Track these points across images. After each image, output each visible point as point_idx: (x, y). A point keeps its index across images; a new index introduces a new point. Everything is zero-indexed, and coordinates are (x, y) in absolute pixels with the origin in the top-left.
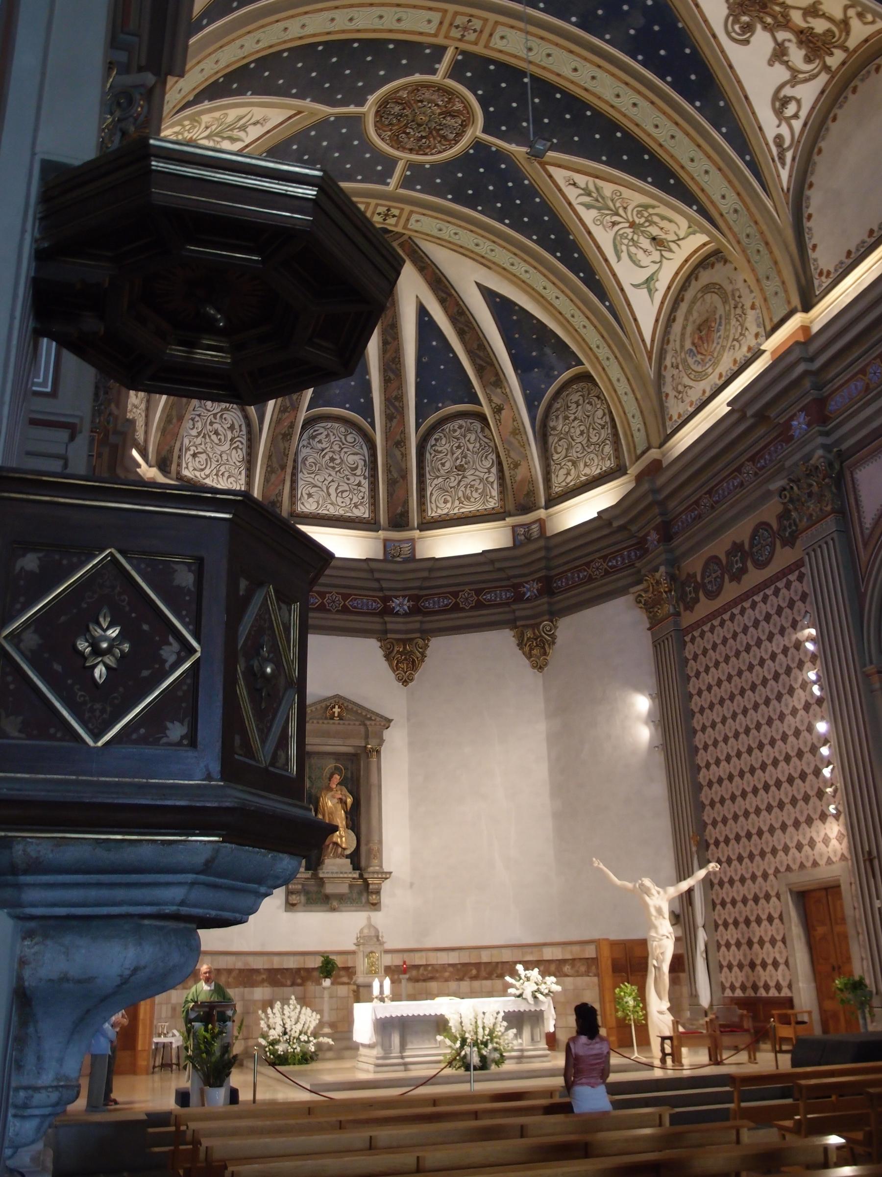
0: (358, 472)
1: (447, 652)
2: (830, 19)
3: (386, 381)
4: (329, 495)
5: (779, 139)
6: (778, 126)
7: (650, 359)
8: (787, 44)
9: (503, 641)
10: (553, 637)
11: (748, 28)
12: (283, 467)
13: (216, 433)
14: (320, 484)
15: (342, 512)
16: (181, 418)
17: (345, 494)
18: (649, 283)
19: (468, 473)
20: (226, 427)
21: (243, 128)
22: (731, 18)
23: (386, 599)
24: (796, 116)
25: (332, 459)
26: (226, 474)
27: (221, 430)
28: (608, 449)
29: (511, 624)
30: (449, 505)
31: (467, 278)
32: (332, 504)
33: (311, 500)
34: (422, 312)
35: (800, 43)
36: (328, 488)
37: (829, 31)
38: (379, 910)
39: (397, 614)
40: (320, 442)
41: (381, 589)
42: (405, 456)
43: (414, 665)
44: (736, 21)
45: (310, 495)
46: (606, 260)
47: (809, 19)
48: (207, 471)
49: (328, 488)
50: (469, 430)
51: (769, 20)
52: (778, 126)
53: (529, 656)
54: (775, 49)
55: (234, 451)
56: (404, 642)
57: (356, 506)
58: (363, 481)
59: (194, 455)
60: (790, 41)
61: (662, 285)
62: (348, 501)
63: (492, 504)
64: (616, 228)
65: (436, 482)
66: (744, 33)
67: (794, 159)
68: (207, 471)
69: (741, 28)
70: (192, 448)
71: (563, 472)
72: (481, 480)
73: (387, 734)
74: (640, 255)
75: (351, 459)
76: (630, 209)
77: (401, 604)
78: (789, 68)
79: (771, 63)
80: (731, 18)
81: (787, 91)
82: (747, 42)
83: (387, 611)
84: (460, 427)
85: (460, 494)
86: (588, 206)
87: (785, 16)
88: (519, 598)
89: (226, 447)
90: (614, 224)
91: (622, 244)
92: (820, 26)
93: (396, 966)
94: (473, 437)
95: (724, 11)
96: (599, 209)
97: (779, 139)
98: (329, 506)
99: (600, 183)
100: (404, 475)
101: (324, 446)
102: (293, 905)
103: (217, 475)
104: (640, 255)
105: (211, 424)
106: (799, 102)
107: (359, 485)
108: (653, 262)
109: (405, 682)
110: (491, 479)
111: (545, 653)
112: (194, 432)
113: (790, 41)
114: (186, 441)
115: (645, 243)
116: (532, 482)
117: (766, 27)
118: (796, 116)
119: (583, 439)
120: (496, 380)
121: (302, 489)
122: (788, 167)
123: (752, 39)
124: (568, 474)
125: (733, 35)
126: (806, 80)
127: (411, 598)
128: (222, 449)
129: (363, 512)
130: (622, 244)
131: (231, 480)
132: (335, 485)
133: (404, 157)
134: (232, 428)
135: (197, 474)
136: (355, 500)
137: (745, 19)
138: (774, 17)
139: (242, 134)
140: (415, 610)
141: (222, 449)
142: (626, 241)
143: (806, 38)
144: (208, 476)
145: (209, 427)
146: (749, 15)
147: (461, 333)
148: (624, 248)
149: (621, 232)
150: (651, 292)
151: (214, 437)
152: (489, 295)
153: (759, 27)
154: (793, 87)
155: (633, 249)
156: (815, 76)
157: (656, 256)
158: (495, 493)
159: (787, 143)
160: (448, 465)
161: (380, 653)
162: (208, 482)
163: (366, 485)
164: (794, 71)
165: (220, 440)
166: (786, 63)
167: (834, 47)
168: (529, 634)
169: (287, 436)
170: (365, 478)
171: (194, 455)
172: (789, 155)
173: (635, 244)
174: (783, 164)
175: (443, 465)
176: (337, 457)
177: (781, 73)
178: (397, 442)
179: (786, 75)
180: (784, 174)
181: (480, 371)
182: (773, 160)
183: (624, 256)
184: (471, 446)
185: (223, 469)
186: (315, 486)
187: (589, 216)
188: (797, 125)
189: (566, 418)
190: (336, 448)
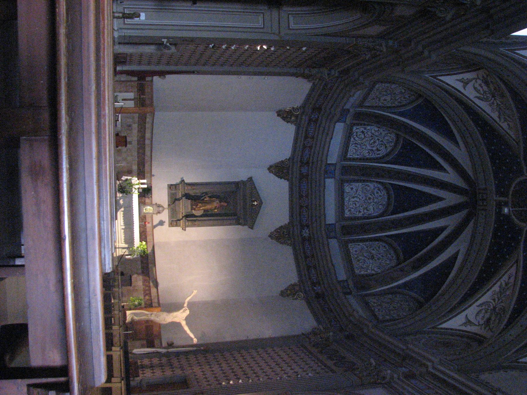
0: (365, 211)
3: (408, 218)
4: (353, 198)
7: (433, 328)
9: (293, 278)
10: (296, 299)
12: (363, 175)
13: (374, 142)
15: (346, 204)
16: (378, 123)
17: (354, 205)
18: (468, 322)
19: (371, 261)
20: (378, 147)
21: (505, 120)
23: (308, 226)
25: (370, 199)
26: (357, 148)
27: (376, 144)
28: (388, 317)
29: (301, 281)
30: (354, 252)
31: (460, 246)
32: (349, 199)
33: (350, 190)
36: (356, 197)
38: (169, 226)
40: (377, 193)
41: (312, 224)
42: (376, 232)
43: (278, 239)
45: (352, 189)
46: (477, 300)
48: (357, 139)
49: (356, 197)
50: (390, 260)
53: (286, 289)
55: (367, 151)
56: (289, 234)
57: (350, 210)
58: (361, 213)
61: (469, 328)
62: (351, 206)
63: (357, 272)
64: (492, 301)
65: (365, 247)
68: (357, 139)
70: (366, 131)
71: (375, 301)
72: (368, 266)
73: (246, 227)
74: (481, 315)
75: (371, 207)
76: (502, 304)
77: (306, 233)
83: (302, 227)
84: (393, 257)
85: (360, 257)
86: (500, 287)
88: (314, 284)
89: (369, 148)
90: (494, 300)
91: (485, 306)
93: (146, 229)
94: (388, 262)
96: (500, 292)
98: (348, 198)
99: (512, 288)
100: (365, 232)
101: (375, 194)
102: (170, 188)
103: (356, 144)
104: (481, 315)
105: (378, 139)
107: (360, 212)
108: (479, 322)
109: (270, 236)
110: (368, 271)
111: (288, 296)
112: (373, 132)
114: (369, 128)
115: (487, 316)
116: (369, 289)
119: (391, 308)
120: (416, 268)
121: (355, 185)
124: (374, 303)
127: (310, 237)
128: (368, 145)
129: (347, 214)
130: (485, 306)
131: (354, 151)
132: (358, 200)
134: (378, 150)
135: (355, 134)
139: (502, 120)
140: (304, 239)
141: (368, 145)
142: (487, 307)
144: (354, 139)
145: (376, 138)
147: (435, 248)
148: (484, 307)
149: (491, 304)
150: (465, 324)
151: (372, 141)
152: (454, 257)
155: (484, 311)
157: (482, 322)
158: (362, 273)
162: (352, 139)
163: (360, 215)
165: (371, 144)
168: (297, 288)
169: (378, 175)
170: (363, 214)
171: (363, 132)
173: (486, 312)
175: (373, 250)
176: (371, 201)
178: (383, 227)
181: (418, 260)
184: (383, 262)
185: (359, 146)
186: (357, 191)
187: (496, 288)
189: (402, 301)
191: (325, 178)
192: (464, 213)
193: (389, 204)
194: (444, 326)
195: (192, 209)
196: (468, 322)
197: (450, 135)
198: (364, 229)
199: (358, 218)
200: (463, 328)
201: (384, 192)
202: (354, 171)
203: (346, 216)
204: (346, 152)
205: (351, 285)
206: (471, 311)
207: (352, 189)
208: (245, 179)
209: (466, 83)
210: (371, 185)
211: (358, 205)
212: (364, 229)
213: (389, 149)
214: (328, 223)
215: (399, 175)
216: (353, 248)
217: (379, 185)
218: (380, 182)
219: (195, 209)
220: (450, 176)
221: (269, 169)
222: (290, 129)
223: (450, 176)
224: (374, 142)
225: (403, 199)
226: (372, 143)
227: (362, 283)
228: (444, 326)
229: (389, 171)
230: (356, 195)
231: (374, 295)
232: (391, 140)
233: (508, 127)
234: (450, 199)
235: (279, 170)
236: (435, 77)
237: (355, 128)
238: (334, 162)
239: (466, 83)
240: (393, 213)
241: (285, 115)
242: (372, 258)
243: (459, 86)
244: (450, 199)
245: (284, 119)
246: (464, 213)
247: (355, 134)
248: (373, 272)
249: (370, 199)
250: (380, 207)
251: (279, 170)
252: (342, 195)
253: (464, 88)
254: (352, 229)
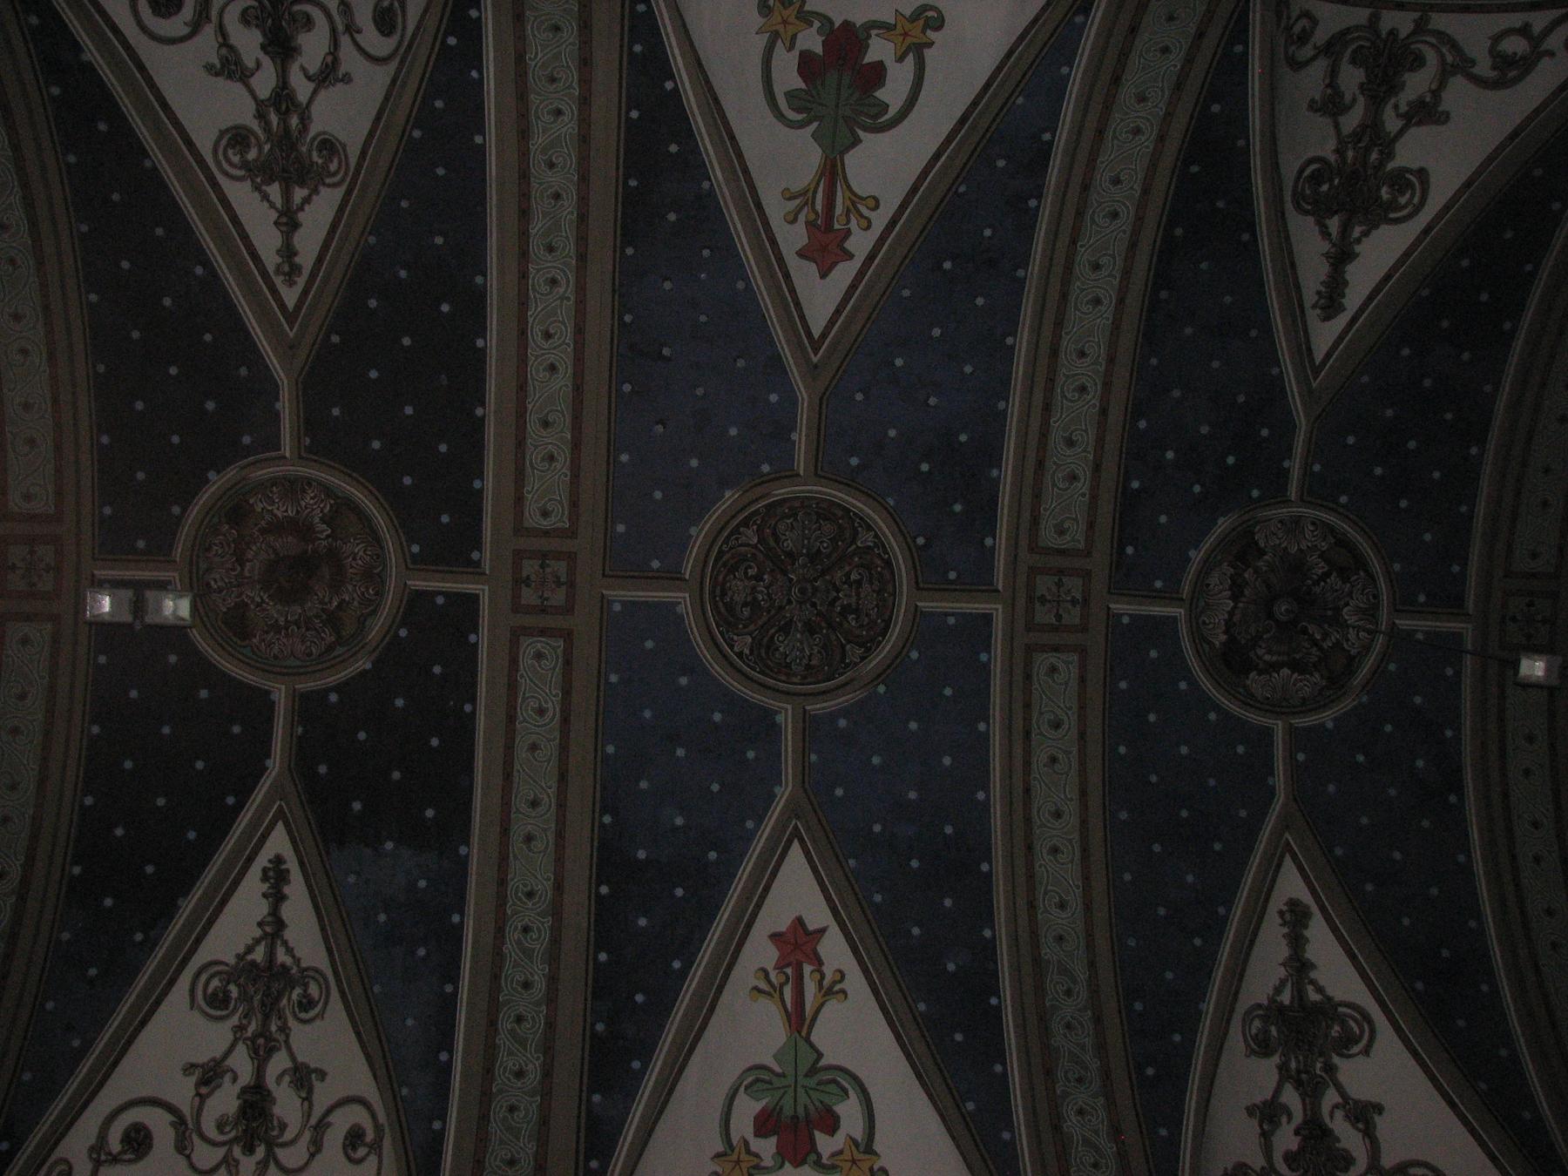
2: (1333, 72)
6: (1551, 54)
8: (1403, 108)
11: (1400, 180)
22: (1392, 215)
35: (1394, 88)
37: (1353, 61)
44: (1393, 205)
47: (1348, 98)
51: (1374, 156)
54: (1420, 123)
60: (1396, 107)
66: (1410, 185)
69: (1403, 194)
78: (1442, 84)
79: (1444, 118)
80: (1392, 215)
81: (1484, 68)
82: (1422, 173)
87: (1357, 136)
92: (1352, 78)
95: (1384, 231)
106: (1497, 39)
113: (1396, 107)
117: (1388, 154)
118: (1524, 31)
123: (1415, 166)
125: (1416, 200)
126: (1454, 45)
137: (1385, 193)
138: (1368, 150)
143: (1382, 86)
146: (1379, 189)
153: (1390, 166)
154: (1473, 62)
156: (1439, 34)
164: (1446, 72)
166: (1436, 94)
167: (1379, 36)
177: (1458, 94)
179: (1458, 83)
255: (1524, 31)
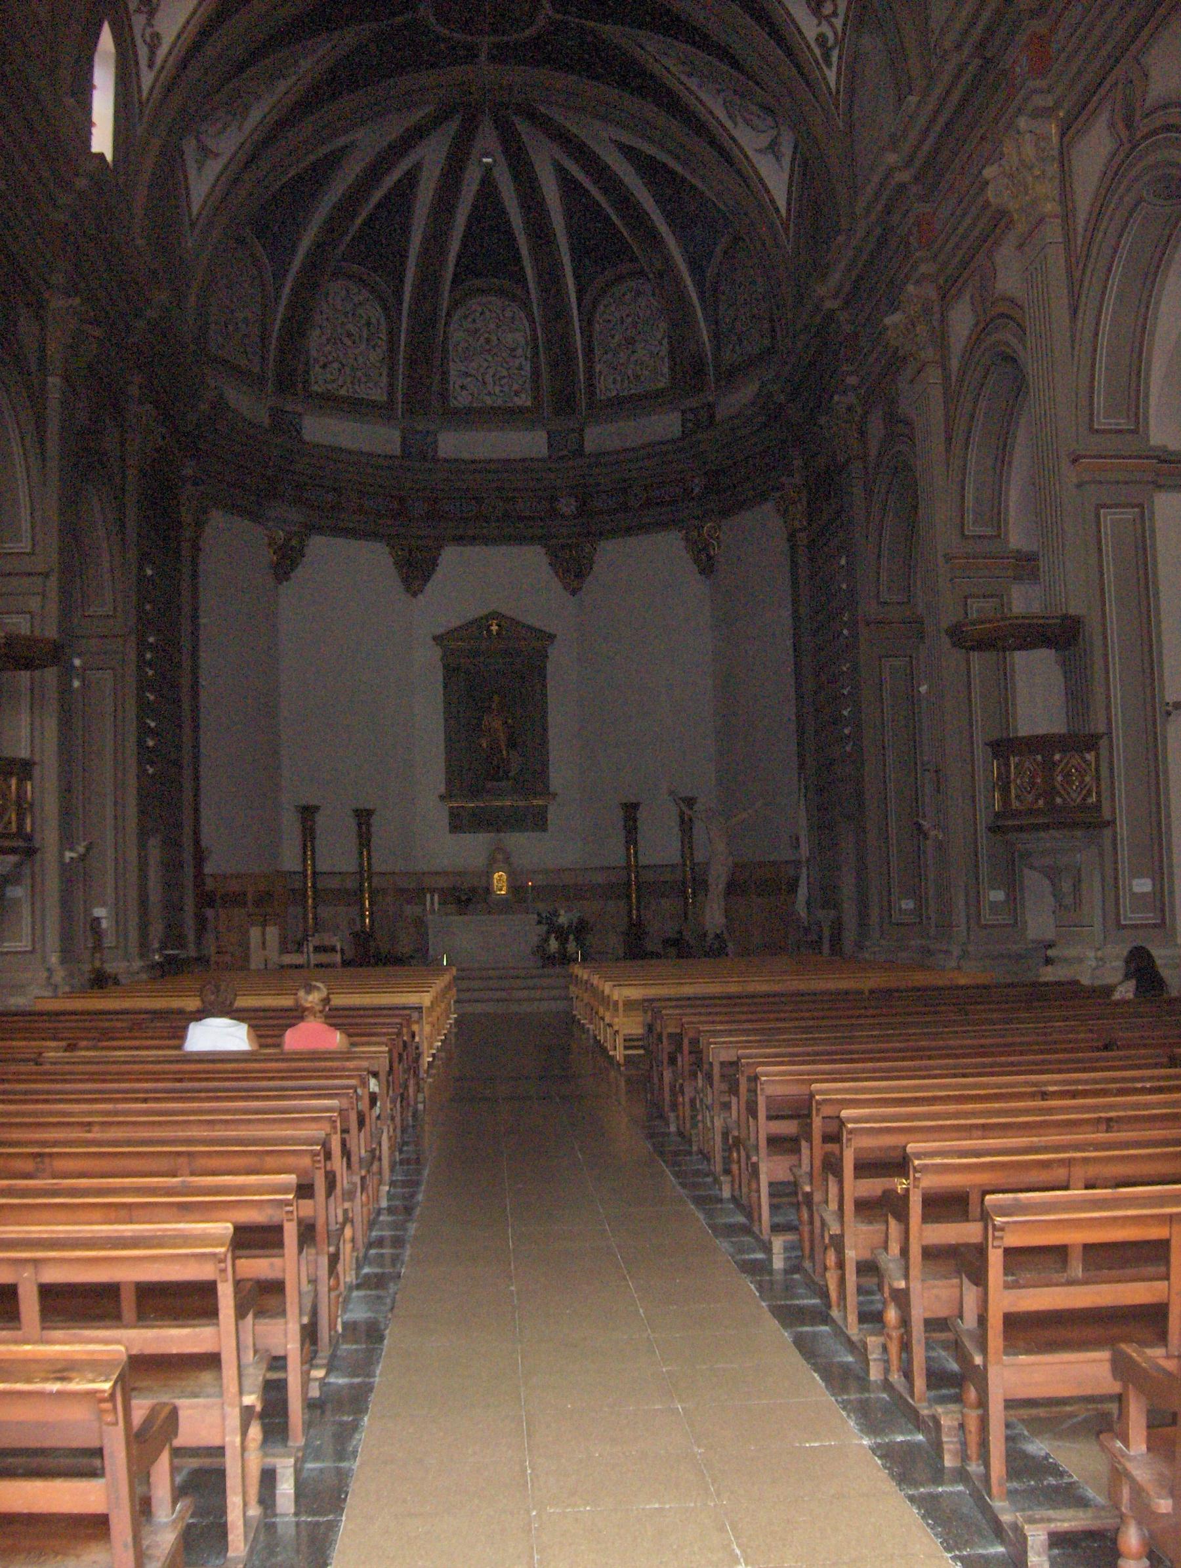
0: (519, 352)
1: (617, 558)
5: (821, 40)
7: (786, 229)
13: (349, 335)
14: (474, 372)
18: (773, 147)
19: (639, 346)
23: (553, 499)
24: (835, 14)
25: (488, 341)
32: (489, 394)
33: (464, 393)
34: (560, 169)
39: (563, 516)
43: (580, 576)
45: (463, 387)
50: (639, 293)
52: (819, 24)
53: (696, 561)
59: (324, 366)
61: (787, 149)
64: (722, 94)
67: (840, 58)
74: (756, 121)
77: (567, 506)
83: (554, 513)
85: (630, 372)
89: (363, 347)
90: (719, 91)
97: (821, 40)
107: (520, 368)
109: (574, 592)
114: (314, 353)
120: (654, 238)
122: (834, 69)
124: (733, 350)
129: (524, 400)
132: (491, 371)
133: (486, 42)
136: (515, 387)
145: (340, 330)
152: (628, 151)
158: (666, 370)
159: (831, 42)
160: (617, 337)
161: (545, 560)
162: (343, 392)
163: (528, 368)
171: (324, 366)
172: (835, 55)
174: (829, 65)
175: (613, 337)
178: (556, 312)
180: (831, 75)
182: (818, 63)
183: (739, 120)
187: (693, 83)
188: (838, 23)
190: (492, 326)
191: (435, 460)
192: (522, 126)
193: (501, 292)
194: (782, 204)
195: (508, 778)
196: (773, 147)
197: (333, 161)
198: (562, 360)
199: (536, 373)
200: (786, 161)
201: (474, 303)
202: (421, 384)
203: (529, 404)
204: (373, 405)
205: (692, 402)
206: (749, 139)
207: (463, 387)
208: (437, 652)
209: (206, 152)
210: (458, 336)
211: (505, 373)
212: (562, 360)
213: (365, 293)
214: (545, 452)
215: (428, 281)
216: (608, 387)
217: (456, 318)
218: (448, 314)
219: (507, 773)
220: (432, 155)
221: (415, 595)
222: (318, 544)
223: (432, 155)
224: (349, 335)
225: (488, 258)
226: (350, 341)
227: (690, 373)
228: (782, 204)
229: (417, 301)
230: (480, 378)
231: (718, 348)
232: (344, 292)
233: (308, 63)
234: (487, 155)
235: (416, 571)
236: (193, 225)
237: (315, 388)
238: (396, 435)
239: (206, 152)
240: (522, 281)
241: (286, 561)
242: (630, 342)
243: (213, 168)
244: (487, 155)
245: (294, 564)
246: (522, 126)
247: (329, 387)
248: (665, 342)
249: (488, 341)
250: (508, 314)
251: (416, 571)
252: (480, 412)
253: (217, 155)
254: (564, 394)
255: (835, 14)
